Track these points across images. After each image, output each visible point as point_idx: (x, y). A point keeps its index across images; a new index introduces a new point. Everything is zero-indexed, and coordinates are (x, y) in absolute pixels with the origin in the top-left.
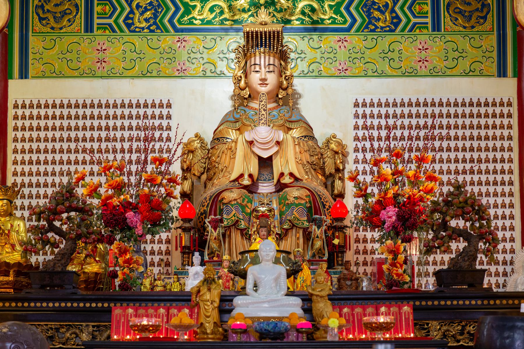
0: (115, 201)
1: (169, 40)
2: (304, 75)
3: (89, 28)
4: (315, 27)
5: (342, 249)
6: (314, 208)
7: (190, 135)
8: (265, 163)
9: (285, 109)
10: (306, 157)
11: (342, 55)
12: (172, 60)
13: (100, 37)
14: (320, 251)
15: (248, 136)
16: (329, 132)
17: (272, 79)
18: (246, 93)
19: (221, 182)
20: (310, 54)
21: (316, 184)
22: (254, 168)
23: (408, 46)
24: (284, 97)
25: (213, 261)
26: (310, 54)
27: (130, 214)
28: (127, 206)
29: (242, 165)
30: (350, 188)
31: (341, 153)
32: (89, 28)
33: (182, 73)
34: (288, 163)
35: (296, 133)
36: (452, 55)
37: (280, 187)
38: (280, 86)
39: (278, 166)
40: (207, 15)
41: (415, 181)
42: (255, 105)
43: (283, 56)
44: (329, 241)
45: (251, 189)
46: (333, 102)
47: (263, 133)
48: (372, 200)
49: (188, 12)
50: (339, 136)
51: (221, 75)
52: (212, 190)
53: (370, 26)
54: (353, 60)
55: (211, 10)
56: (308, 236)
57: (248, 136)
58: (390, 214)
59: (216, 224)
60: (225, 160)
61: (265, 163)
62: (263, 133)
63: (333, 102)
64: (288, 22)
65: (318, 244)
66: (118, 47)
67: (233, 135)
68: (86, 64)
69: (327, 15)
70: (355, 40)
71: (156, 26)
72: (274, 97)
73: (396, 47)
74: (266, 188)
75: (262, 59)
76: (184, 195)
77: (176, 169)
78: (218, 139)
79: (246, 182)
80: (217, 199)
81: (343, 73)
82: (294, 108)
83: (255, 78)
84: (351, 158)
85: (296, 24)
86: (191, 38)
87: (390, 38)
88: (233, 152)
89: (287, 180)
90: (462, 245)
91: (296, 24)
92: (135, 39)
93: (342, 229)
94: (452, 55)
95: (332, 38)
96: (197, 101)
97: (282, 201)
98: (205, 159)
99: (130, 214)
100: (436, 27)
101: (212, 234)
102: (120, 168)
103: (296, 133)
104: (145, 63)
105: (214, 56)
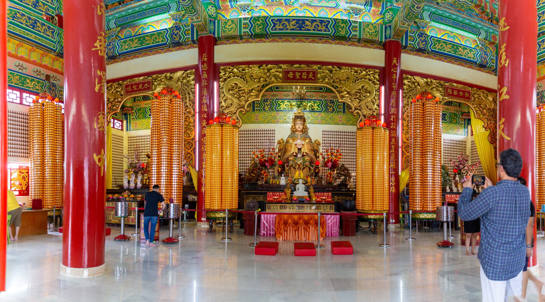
0: (263, 160)
1: (274, 113)
2: (309, 123)
3: (254, 110)
4: (313, 110)
5: (318, 173)
6: (311, 162)
7: (280, 139)
8: (299, 149)
9: (304, 134)
10: (310, 148)
11: (319, 118)
12: (275, 119)
13: (257, 113)
14: (313, 173)
15: (295, 143)
16: (316, 138)
17: (301, 127)
18: (295, 130)
19: (288, 154)
20: (311, 118)
21: (312, 155)
22: (297, 151)
23: (336, 116)
24: (305, 131)
25: (287, 176)
26: (311, 118)
27: (266, 163)
28: (265, 161)
29: (294, 150)
30: (321, 157)
31: (319, 144)
32: (254, 110)
33: (278, 122)
34: (305, 150)
35: (307, 141)
36: (348, 119)
37: (303, 156)
38: (303, 128)
39: (303, 150)
40: (284, 107)
41: (336, 156)
42: (297, 133)
43: (304, 121)
44: (315, 170)
45: (296, 156)
46: (317, 131)
47: (299, 142)
48: (326, 160)
49: (279, 106)
50: (319, 140)
51: (288, 123)
52: (286, 156)
53: (327, 110)
54: (322, 120)
55: (286, 105)
56: (310, 169)
57: (295, 143)
58: (330, 164)
59: (287, 166)
60: (289, 148)
61: (299, 149)
62: (299, 142)
63: (317, 131)
64: (306, 109)
65: (312, 171)
66: (261, 115)
67: (291, 141)
68: (253, 120)
69: (316, 107)
70: (323, 114)
71: (271, 109)
72: (302, 131)
73: (334, 117)
74: (299, 155)
75: (299, 122)
76: (279, 156)
77: (277, 151)
78: (287, 142)
79: (295, 154)
80: (287, 159)
81: (320, 123)
82: (307, 134)
83: (297, 127)
84: (322, 145)
85: (308, 109)
86: (280, 113)
87: (332, 114)
88: (291, 146)
89: (305, 154)
90: (343, 177)
91: (308, 109)
92: (266, 114)
93: (318, 168)
94: (348, 119)
95: (317, 113)
96: (282, 130)
97: (304, 159)
98: (284, 147)
99: (266, 163)
100: (344, 112)
101: (287, 168)
102: (264, 151)
103: (307, 141)
104: (268, 119)
105: (286, 118)
